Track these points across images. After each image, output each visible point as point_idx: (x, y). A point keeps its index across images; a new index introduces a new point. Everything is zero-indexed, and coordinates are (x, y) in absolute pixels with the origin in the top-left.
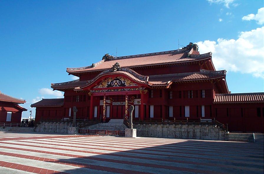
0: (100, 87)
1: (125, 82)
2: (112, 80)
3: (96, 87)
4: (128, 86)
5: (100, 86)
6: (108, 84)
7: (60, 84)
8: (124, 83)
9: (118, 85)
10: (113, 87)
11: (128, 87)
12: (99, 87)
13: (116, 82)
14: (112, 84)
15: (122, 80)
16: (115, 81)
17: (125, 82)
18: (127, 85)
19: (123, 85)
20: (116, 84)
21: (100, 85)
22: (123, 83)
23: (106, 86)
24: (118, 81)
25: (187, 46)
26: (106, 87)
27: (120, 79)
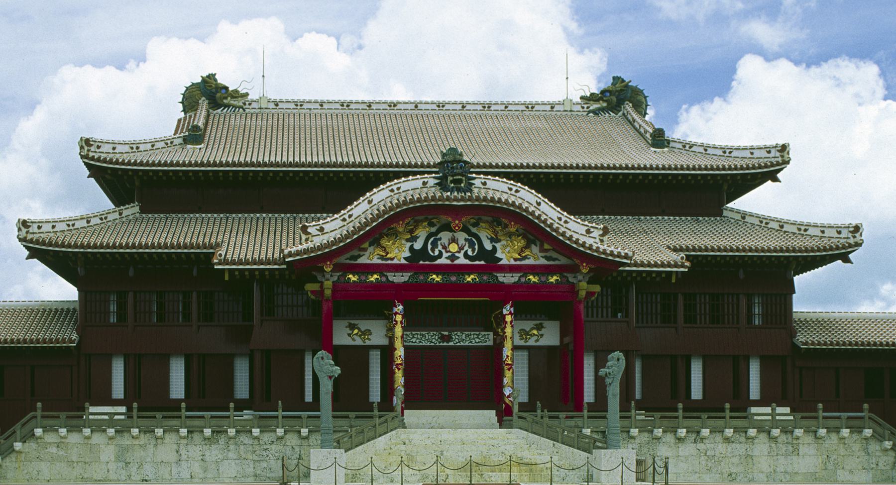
0: (371, 257)
1: (498, 245)
2: (433, 230)
3: (348, 255)
4: (513, 262)
5: (367, 253)
6: (411, 249)
7: (78, 225)
8: (494, 248)
9: (461, 255)
10: (439, 262)
11: (512, 269)
12: (363, 260)
13: (454, 240)
14: (433, 251)
15: (484, 235)
16: (445, 236)
17: (498, 245)
18: (506, 255)
19: (490, 256)
20: (454, 248)
21: (371, 249)
22: (488, 246)
23: (399, 253)
24: (462, 236)
25: (603, 92)
26: (404, 262)
27: (475, 225)
